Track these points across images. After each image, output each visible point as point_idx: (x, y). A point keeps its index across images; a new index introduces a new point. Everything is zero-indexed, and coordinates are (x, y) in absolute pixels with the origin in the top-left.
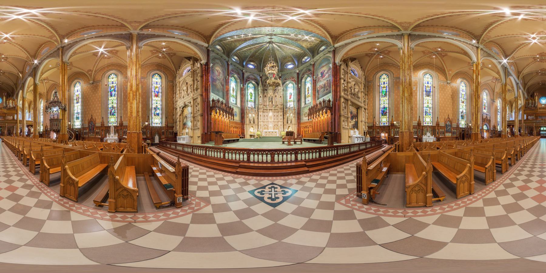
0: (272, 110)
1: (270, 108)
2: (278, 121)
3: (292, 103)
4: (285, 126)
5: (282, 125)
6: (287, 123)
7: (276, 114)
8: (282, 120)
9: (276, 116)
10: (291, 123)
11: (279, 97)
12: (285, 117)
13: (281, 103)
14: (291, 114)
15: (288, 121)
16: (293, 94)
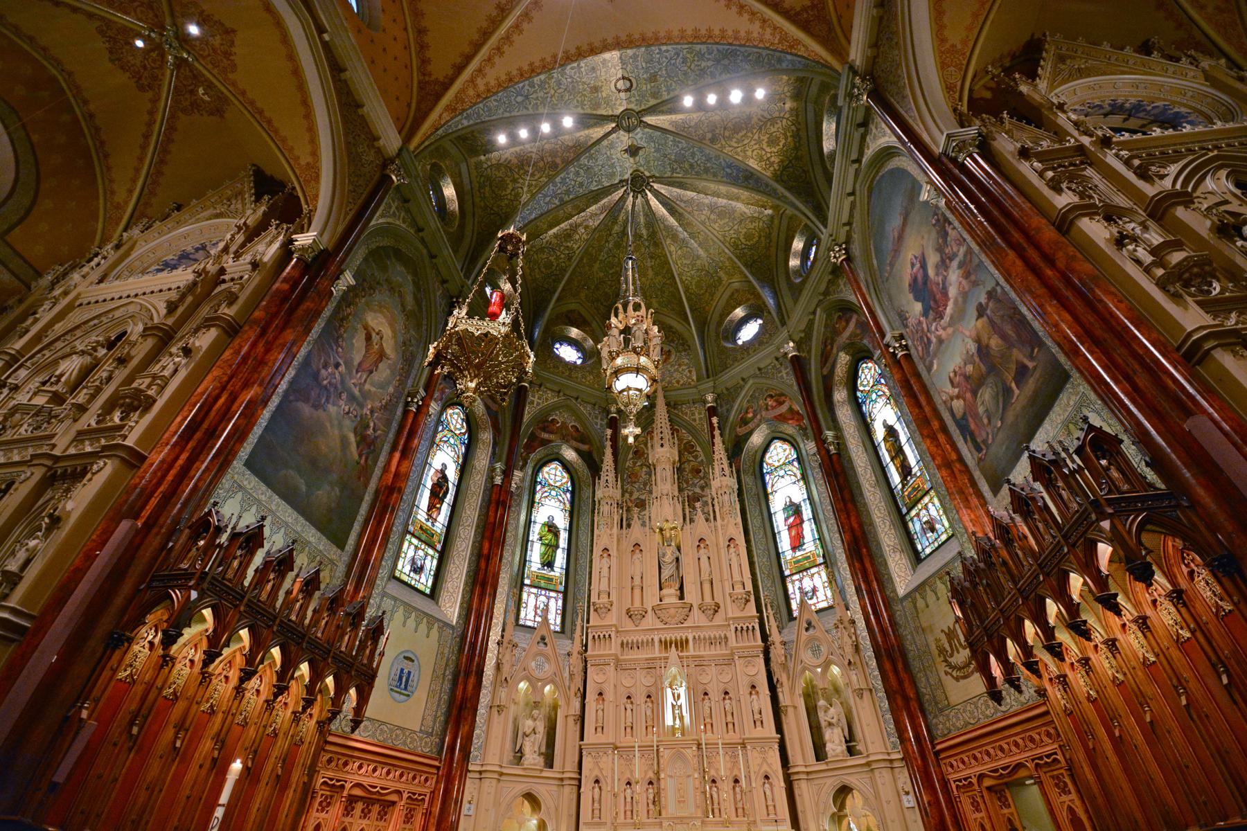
0: (682, 644)
1: (669, 636)
2: (733, 737)
3: (818, 580)
4: (804, 790)
5: (780, 784)
6: (820, 753)
7: (713, 679)
8: (770, 730)
9: (715, 695)
10: (851, 751)
11: (723, 542)
12: (784, 699)
13: (739, 590)
14: (835, 670)
15: (828, 734)
16: (807, 513)
